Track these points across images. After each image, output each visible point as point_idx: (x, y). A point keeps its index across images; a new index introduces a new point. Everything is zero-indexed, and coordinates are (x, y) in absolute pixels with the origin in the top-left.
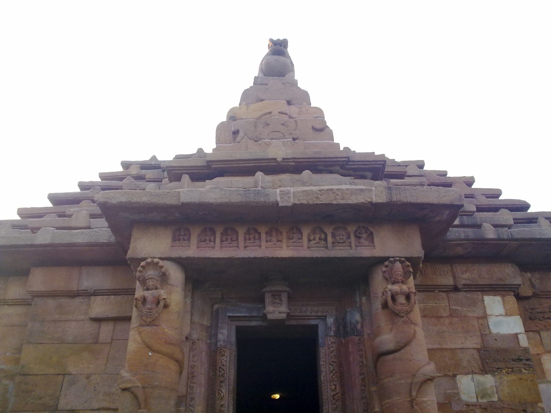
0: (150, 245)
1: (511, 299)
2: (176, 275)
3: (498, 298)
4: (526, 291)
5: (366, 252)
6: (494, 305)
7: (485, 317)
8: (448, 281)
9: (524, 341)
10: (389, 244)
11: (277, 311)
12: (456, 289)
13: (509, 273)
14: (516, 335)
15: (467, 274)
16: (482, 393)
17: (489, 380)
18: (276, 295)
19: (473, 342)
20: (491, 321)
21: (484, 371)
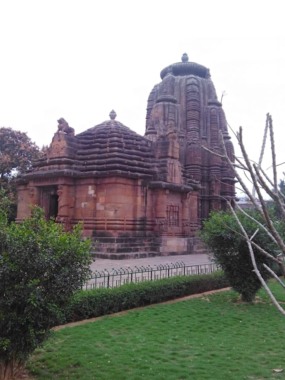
0: (31, 184)
1: (93, 186)
2: (35, 189)
3: (91, 186)
4: (99, 184)
5: (57, 184)
6: (90, 187)
7: (88, 190)
8: (82, 183)
9: (93, 195)
10: (60, 182)
11: (52, 193)
12: (84, 185)
13: (92, 181)
14: (92, 194)
15: (86, 182)
16: (85, 205)
17: (86, 203)
18: (52, 190)
19: (85, 196)
20: (89, 191)
21: (86, 201)
